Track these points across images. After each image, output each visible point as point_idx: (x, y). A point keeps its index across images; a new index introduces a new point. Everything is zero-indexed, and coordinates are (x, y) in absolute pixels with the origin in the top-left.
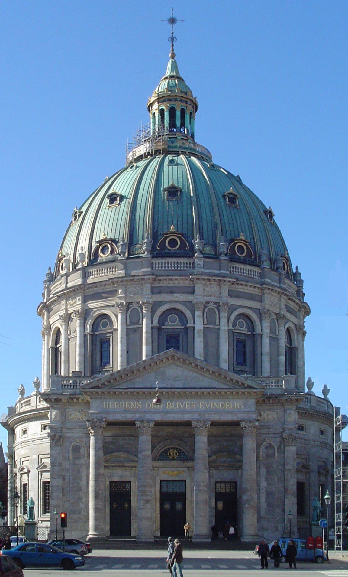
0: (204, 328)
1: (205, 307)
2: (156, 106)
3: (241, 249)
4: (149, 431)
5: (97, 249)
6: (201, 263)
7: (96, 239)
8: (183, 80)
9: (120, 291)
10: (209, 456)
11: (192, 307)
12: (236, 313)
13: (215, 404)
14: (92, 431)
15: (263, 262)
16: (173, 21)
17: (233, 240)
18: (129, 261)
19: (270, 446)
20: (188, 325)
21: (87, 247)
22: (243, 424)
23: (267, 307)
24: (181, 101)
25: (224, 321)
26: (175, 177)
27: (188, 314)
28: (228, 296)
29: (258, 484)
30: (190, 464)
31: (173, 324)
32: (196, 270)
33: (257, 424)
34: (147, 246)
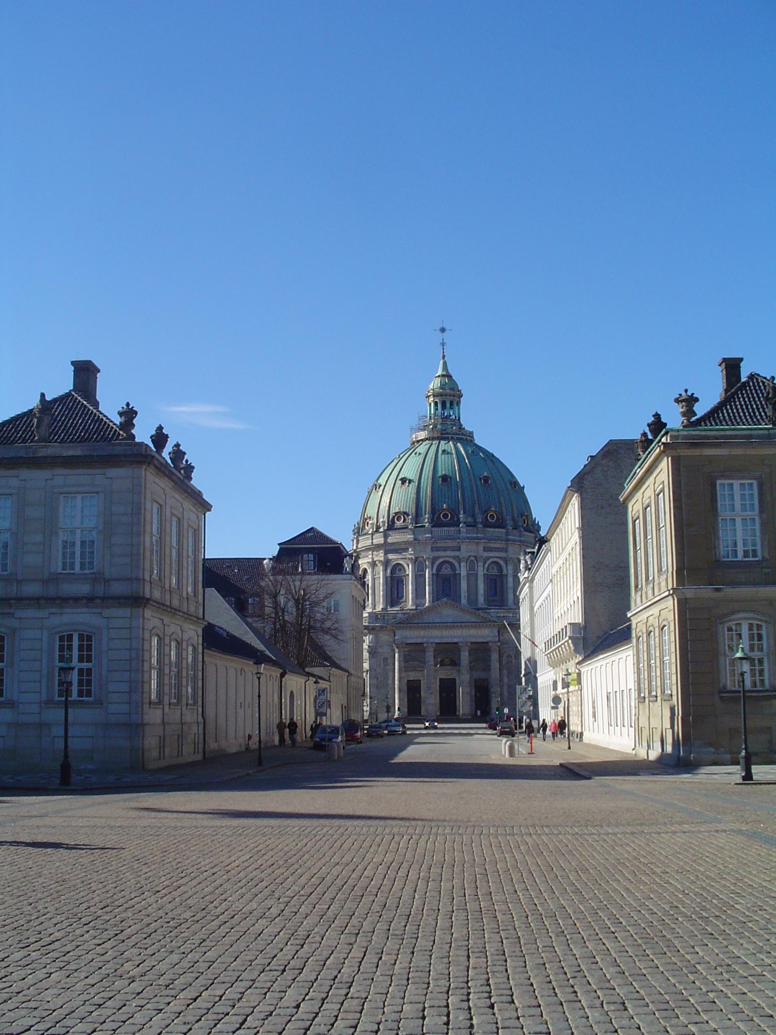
0: (468, 574)
1: (468, 559)
2: (431, 399)
3: (492, 516)
4: (432, 649)
5: (394, 517)
6: (465, 530)
7: (392, 511)
8: (451, 377)
9: (410, 550)
10: (470, 663)
11: (459, 561)
12: (489, 562)
13: (473, 632)
14: (397, 650)
15: (507, 525)
16: (443, 330)
17: (486, 511)
18: (417, 529)
19: (509, 656)
20: (457, 572)
21: (386, 515)
22: (490, 644)
23: (511, 556)
24: (450, 396)
25: (481, 569)
26: (446, 465)
27: (456, 564)
28: (482, 551)
29: (501, 680)
30: (458, 668)
31: (446, 571)
32: (462, 535)
33: (499, 644)
34: (428, 520)
